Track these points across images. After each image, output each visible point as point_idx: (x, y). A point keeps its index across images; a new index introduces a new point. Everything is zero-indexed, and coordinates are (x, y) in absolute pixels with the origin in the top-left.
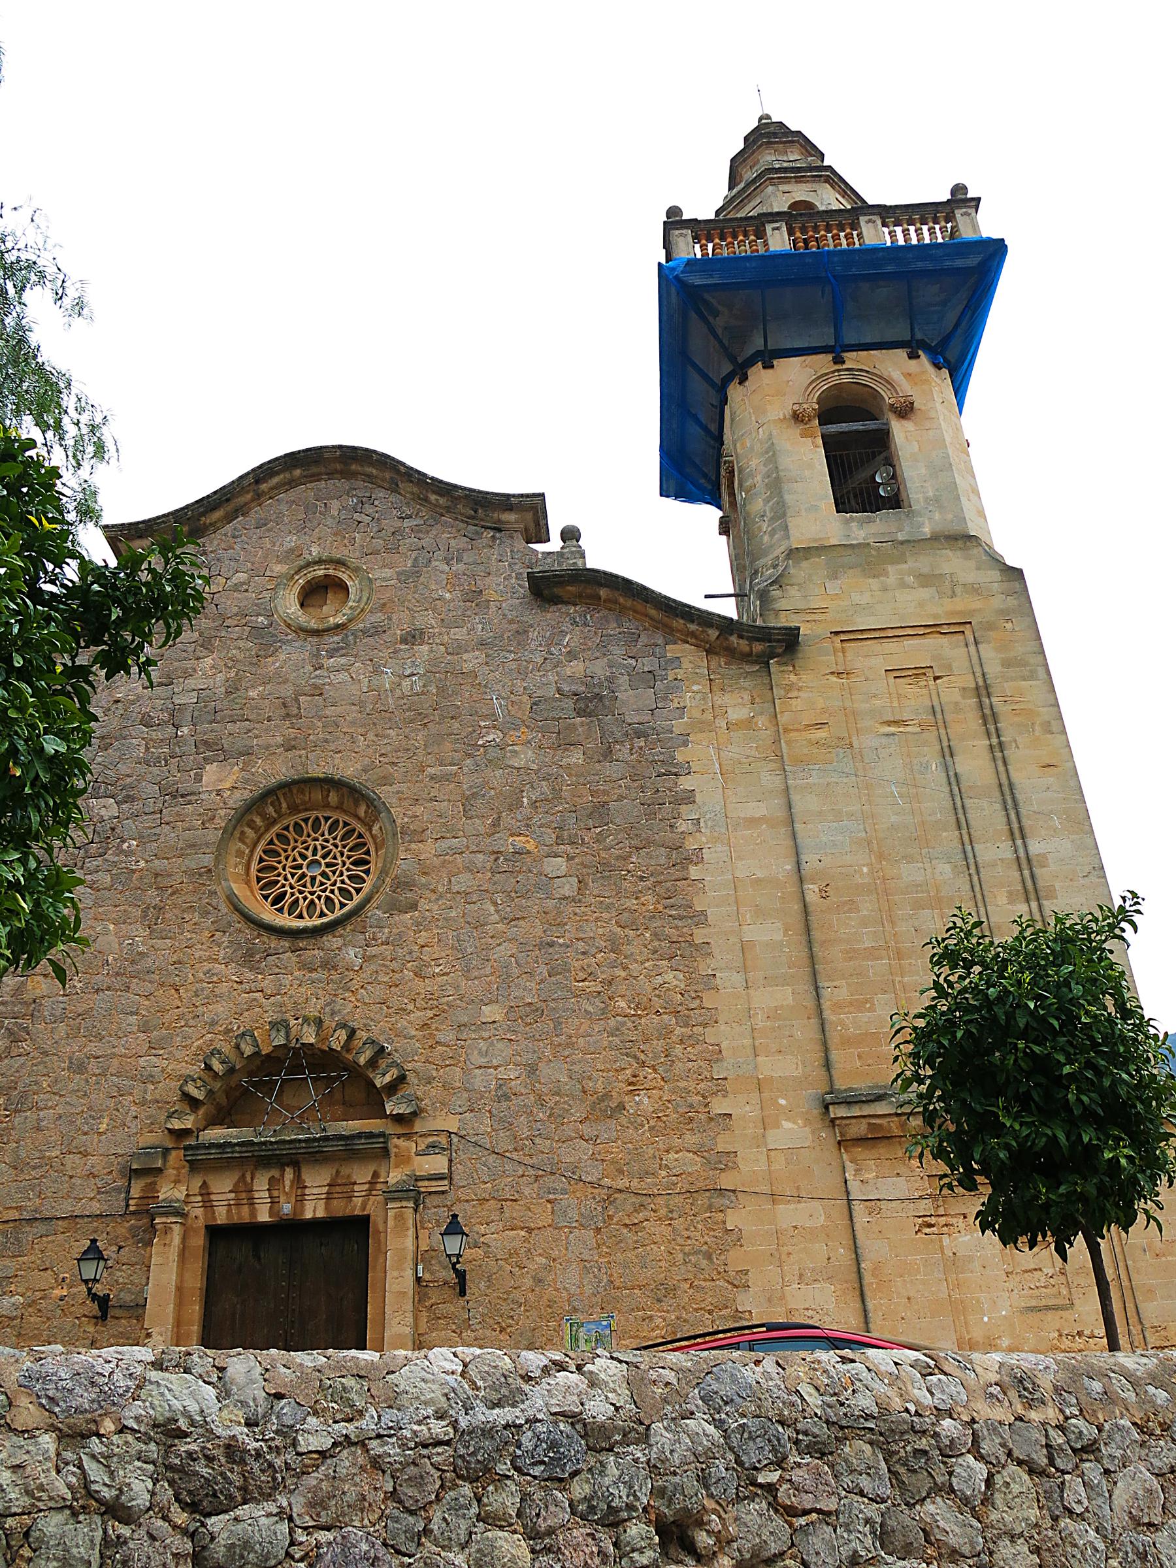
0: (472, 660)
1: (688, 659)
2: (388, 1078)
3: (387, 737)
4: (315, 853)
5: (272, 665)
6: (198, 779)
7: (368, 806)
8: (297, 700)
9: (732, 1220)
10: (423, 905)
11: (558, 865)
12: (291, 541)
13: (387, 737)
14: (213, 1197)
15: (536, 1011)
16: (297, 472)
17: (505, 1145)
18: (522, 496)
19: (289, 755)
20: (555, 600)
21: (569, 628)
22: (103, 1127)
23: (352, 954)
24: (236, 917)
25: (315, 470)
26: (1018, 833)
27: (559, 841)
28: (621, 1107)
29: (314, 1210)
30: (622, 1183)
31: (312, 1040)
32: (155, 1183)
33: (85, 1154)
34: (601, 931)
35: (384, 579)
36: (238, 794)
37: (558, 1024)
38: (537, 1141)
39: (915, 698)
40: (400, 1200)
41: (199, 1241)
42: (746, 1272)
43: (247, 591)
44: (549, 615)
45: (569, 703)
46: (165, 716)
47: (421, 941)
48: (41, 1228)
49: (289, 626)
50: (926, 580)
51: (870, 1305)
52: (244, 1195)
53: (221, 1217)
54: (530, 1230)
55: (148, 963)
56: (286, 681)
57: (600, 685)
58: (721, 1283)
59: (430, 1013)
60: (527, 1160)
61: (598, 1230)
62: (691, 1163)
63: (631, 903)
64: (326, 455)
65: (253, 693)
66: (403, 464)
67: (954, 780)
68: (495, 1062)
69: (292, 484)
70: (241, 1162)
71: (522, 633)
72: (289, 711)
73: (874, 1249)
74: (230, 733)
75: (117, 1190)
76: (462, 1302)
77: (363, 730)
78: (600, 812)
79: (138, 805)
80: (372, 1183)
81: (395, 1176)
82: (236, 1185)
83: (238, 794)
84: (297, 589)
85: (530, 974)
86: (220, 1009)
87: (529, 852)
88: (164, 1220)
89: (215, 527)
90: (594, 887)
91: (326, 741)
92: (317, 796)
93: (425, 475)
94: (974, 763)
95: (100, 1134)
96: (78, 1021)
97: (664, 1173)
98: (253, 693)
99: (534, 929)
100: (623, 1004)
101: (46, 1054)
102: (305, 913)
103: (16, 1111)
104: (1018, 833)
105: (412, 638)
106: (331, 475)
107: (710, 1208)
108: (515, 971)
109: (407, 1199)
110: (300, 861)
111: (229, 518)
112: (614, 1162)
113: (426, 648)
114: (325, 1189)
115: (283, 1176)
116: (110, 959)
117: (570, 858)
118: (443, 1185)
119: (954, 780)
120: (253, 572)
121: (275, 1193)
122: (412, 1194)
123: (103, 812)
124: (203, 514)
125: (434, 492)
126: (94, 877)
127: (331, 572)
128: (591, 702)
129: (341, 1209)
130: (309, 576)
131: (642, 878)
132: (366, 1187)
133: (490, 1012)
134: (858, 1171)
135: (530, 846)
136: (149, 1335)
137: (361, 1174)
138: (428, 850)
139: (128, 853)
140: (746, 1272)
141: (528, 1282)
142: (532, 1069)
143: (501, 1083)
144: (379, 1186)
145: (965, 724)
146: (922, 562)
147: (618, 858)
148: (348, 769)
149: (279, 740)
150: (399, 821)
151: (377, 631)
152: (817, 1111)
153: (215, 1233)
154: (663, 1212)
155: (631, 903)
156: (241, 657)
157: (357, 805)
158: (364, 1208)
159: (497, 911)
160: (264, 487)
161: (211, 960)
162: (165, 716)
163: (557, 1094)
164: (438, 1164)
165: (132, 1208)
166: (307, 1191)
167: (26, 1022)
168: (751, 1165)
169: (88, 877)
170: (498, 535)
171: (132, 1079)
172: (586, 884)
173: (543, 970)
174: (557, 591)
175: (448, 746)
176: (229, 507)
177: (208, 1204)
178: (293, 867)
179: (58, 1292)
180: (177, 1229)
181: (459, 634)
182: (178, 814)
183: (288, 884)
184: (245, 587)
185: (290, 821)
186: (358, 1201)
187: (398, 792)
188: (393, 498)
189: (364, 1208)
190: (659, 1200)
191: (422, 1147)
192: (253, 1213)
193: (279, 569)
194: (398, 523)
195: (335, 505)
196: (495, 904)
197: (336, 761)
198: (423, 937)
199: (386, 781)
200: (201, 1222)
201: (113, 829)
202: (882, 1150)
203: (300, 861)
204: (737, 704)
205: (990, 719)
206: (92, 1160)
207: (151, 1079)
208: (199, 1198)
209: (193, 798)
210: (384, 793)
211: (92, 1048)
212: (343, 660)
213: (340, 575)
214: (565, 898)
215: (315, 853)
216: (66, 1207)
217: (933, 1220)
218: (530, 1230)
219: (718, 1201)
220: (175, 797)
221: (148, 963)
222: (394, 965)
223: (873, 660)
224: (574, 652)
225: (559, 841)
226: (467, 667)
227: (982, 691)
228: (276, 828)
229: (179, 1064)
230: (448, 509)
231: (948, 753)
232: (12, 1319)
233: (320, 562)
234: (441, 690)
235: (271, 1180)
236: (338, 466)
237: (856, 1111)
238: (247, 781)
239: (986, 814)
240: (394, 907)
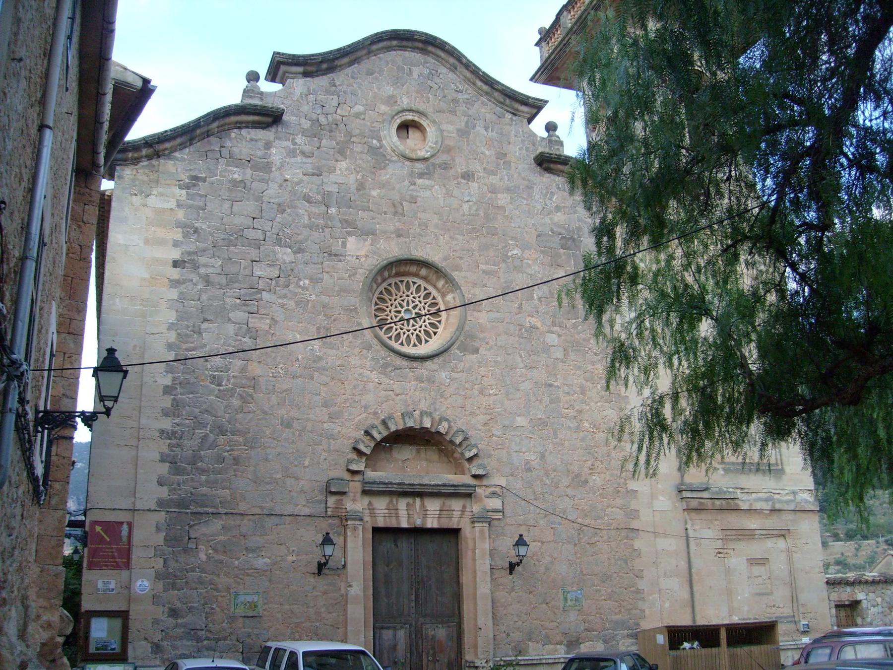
0: (503, 199)
2: (472, 454)
3: (457, 240)
4: (408, 305)
5: (385, 176)
6: (344, 245)
7: (446, 283)
8: (402, 204)
9: (637, 544)
10: (482, 351)
11: (552, 339)
12: (389, 90)
13: (457, 240)
14: (376, 511)
15: (543, 423)
16: (395, 43)
17: (530, 497)
18: (536, 99)
19: (402, 239)
20: (548, 170)
22: (307, 463)
23: (443, 375)
24: (375, 341)
25: (405, 43)
27: (554, 324)
28: (586, 482)
29: (432, 523)
30: (587, 522)
31: (429, 426)
32: (342, 500)
33: (297, 479)
34: (576, 381)
35: (449, 132)
36: (369, 261)
37: (555, 432)
38: (546, 495)
40: (482, 522)
41: (370, 535)
42: (642, 571)
43: (364, 119)
44: (544, 180)
45: (557, 239)
46: (319, 197)
47: (482, 373)
48: (275, 520)
49: (394, 151)
51: (695, 589)
52: (393, 512)
53: (381, 523)
54: (543, 543)
55: (323, 363)
56: (394, 189)
57: (573, 231)
58: (631, 575)
59: (488, 417)
60: (541, 506)
61: (575, 545)
62: (619, 514)
63: (590, 367)
64: (416, 37)
65: (374, 193)
66: (466, 58)
68: (524, 450)
69: (389, 49)
70: (391, 493)
71: (530, 188)
72: (397, 210)
73: (697, 563)
75: (319, 502)
76: (511, 577)
77: (443, 233)
79: (307, 256)
80: (463, 511)
81: (476, 508)
82: (388, 505)
83: (369, 261)
84: (396, 126)
85: (541, 401)
86: (369, 398)
87: (537, 328)
88: (353, 522)
89: (342, 67)
90: (572, 356)
91: (421, 235)
92: (413, 269)
93: (479, 69)
95: (305, 467)
96: (284, 394)
97: (606, 518)
98: (374, 193)
99: (541, 375)
100: (587, 425)
101: (265, 413)
102: (405, 343)
103: (251, 447)
105: (468, 176)
106: (414, 49)
107: (627, 538)
108: (533, 399)
109: (486, 522)
110: (400, 309)
111: (351, 63)
112: (582, 510)
113: (476, 185)
114: (438, 512)
115: (414, 502)
116: (300, 357)
117: (559, 336)
118: (499, 516)
121: (411, 512)
122: (485, 518)
123: (285, 257)
124: (337, 58)
125: (481, 80)
126: (285, 301)
127: (416, 119)
129: (446, 524)
130: (403, 119)
131: (596, 354)
132: (460, 513)
133: (521, 421)
134: (692, 525)
135: (539, 325)
136: (350, 586)
137: (456, 505)
139: (304, 288)
140: (642, 571)
141: (542, 569)
142: (543, 456)
143: (527, 463)
144: (466, 513)
147: (584, 340)
148: (434, 256)
149: (392, 228)
150: (466, 296)
151: (446, 166)
152: (675, 492)
153: (376, 531)
154: (606, 538)
155: (590, 367)
156: (364, 165)
157: (438, 278)
158: (458, 523)
159: (523, 361)
160: (374, 47)
161: (362, 367)
162: (319, 197)
163: (554, 471)
164: (496, 503)
165: (329, 513)
166: (428, 512)
167: (251, 391)
168: (645, 519)
169: (280, 301)
170: (514, 118)
171: (321, 435)
172: (568, 353)
173: (546, 399)
174: (552, 166)
175: (491, 253)
176: (353, 57)
177: (373, 515)
178: (396, 312)
179: (290, 558)
180: (361, 528)
181: (494, 180)
182: (333, 267)
184: (363, 116)
185: (392, 281)
186: (455, 521)
187: (465, 277)
188: (451, 75)
189: (458, 523)
190: (605, 532)
191: (487, 493)
192: (398, 522)
193: (383, 108)
194: (455, 95)
195: (416, 71)
196: (521, 357)
197: (428, 250)
198: (482, 371)
199: (458, 268)
200: (369, 527)
201: (292, 270)
202: (704, 515)
203: (400, 309)
206: (302, 483)
207: (331, 437)
208: (368, 511)
209: (342, 258)
210: (456, 275)
211: (294, 413)
212: (427, 182)
213: (422, 122)
214: (557, 359)
215: (408, 305)
216: (289, 509)
217: (721, 551)
218: (543, 543)
219: (631, 535)
220: (330, 255)
221: (323, 363)
222: (467, 385)
225: (554, 324)
226: (500, 203)
228: (385, 285)
229: (350, 429)
230: (487, 93)
232: (265, 571)
233: (410, 110)
234: (487, 215)
235: (408, 505)
236: (420, 45)
237: (695, 495)
238: (374, 253)
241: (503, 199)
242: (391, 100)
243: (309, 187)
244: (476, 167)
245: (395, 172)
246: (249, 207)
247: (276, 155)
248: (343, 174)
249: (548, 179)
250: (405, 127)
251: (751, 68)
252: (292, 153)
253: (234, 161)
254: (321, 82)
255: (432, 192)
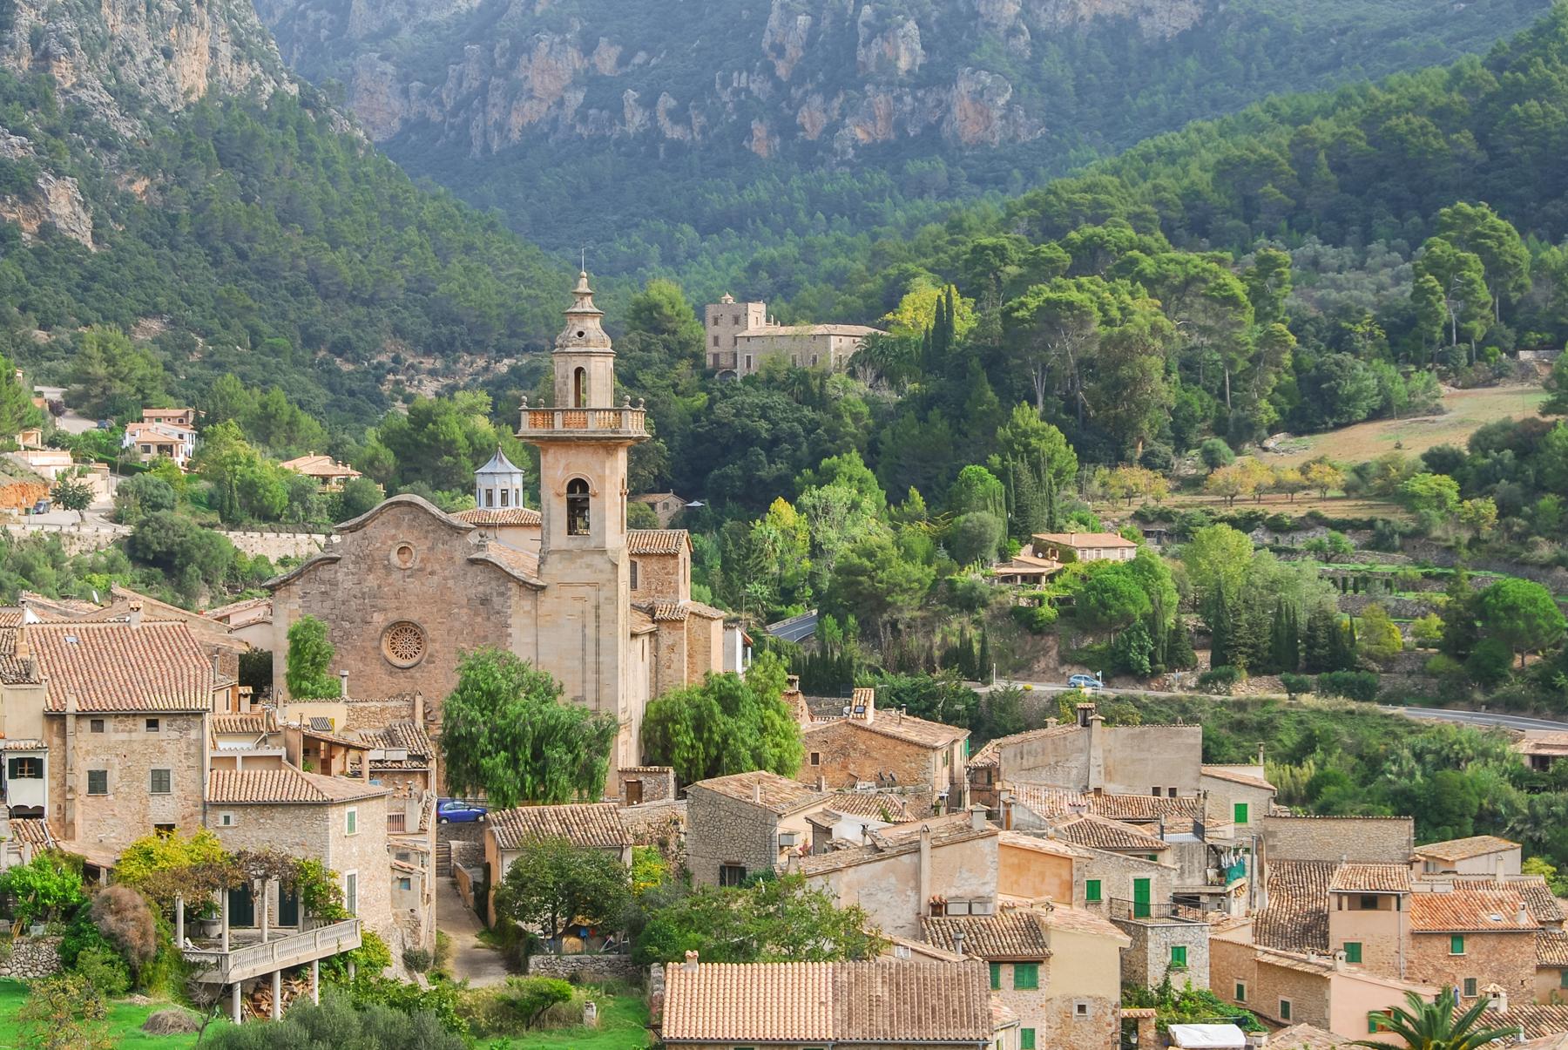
0: (451, 583)
1: (514, 589)
21: (477, 574)
26: (598, 654)
39: (579, 605)
50: (589, 566)
67: (584, 636)
74: (380, 603)
78: (485, 638)
94: (591, 631)
104: (598, 654)
105: (432, 573)
119: (584, 636)
120: (384, 543)
128: (485, 601)
138: (437, 646)
145: (591, 619)
146: (588, 559)
183: (399, 648)
204: (527, 604)
205: (598, 617)
223: (568, 593)
224: (477, 584)
227: (597, 607)
231: (584, 626)
239: (591, 647)
240: (428, 662)
241: (451, 583)
242: (393, 537)
243: (356, 590)
244: (437, 567)
245: (397, 576)
246: (329, 603)
247: (340, 576)
248: (371, 581)
249: (475, 568)
250: (402, 550)
251: (982, 144)
252: (347, 574)
253: (322, 582)
254: (360, 533)
255: (414, 585)
